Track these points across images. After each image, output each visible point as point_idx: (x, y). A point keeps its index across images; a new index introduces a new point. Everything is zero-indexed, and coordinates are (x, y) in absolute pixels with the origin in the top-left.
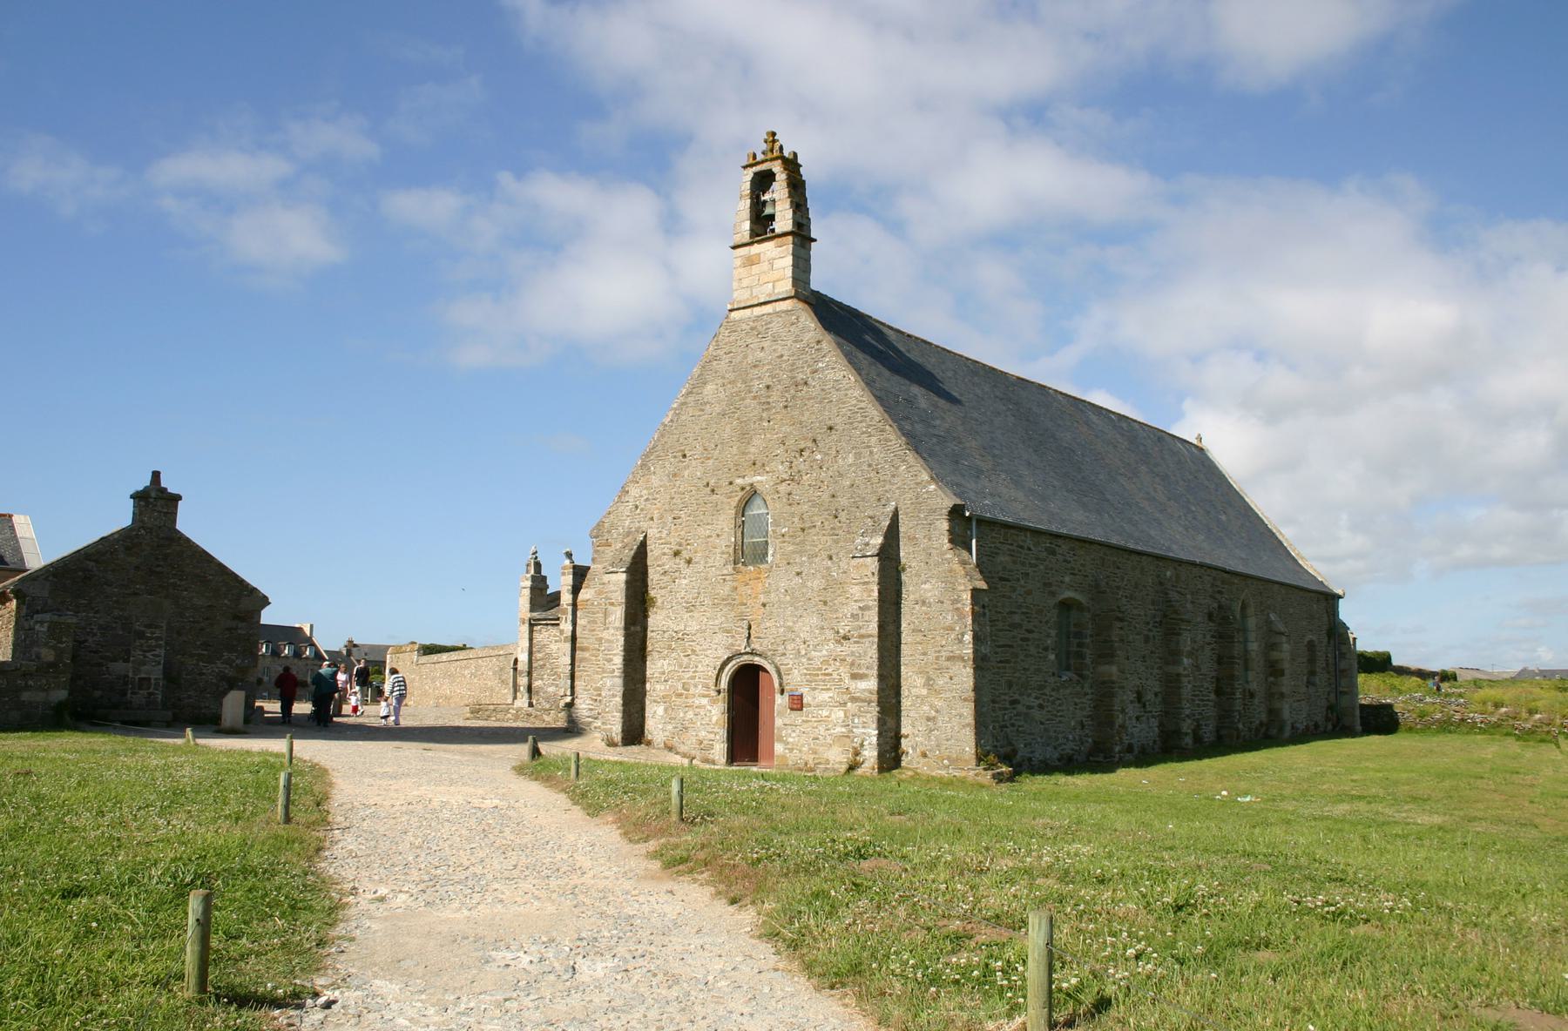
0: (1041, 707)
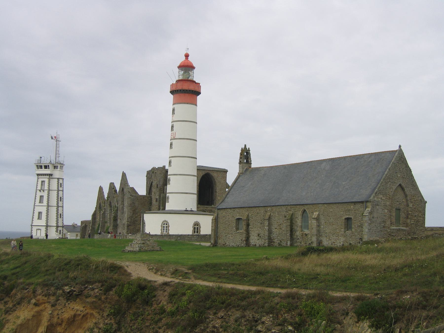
0: (232, 237)
